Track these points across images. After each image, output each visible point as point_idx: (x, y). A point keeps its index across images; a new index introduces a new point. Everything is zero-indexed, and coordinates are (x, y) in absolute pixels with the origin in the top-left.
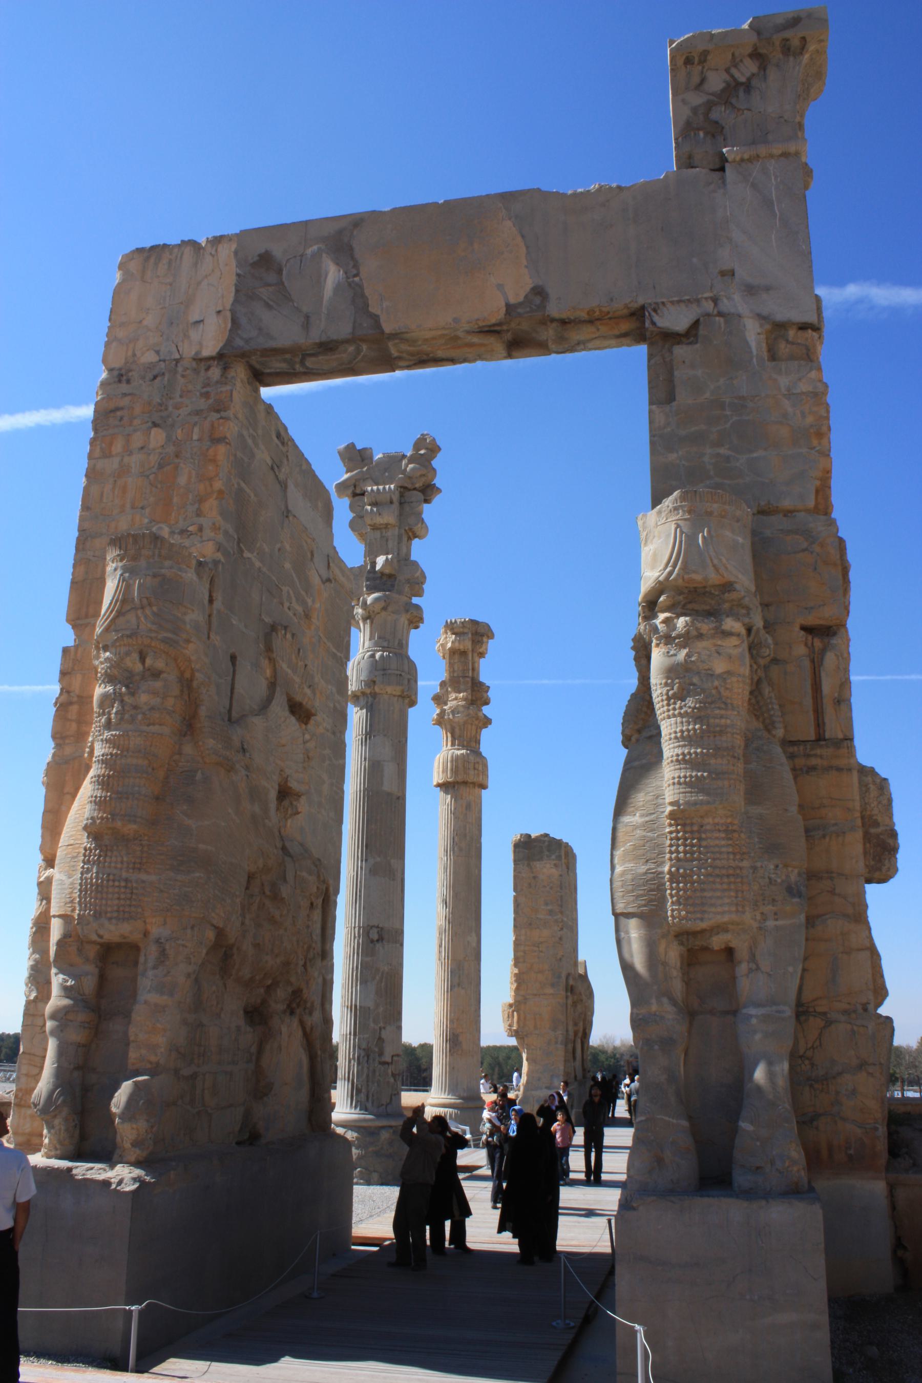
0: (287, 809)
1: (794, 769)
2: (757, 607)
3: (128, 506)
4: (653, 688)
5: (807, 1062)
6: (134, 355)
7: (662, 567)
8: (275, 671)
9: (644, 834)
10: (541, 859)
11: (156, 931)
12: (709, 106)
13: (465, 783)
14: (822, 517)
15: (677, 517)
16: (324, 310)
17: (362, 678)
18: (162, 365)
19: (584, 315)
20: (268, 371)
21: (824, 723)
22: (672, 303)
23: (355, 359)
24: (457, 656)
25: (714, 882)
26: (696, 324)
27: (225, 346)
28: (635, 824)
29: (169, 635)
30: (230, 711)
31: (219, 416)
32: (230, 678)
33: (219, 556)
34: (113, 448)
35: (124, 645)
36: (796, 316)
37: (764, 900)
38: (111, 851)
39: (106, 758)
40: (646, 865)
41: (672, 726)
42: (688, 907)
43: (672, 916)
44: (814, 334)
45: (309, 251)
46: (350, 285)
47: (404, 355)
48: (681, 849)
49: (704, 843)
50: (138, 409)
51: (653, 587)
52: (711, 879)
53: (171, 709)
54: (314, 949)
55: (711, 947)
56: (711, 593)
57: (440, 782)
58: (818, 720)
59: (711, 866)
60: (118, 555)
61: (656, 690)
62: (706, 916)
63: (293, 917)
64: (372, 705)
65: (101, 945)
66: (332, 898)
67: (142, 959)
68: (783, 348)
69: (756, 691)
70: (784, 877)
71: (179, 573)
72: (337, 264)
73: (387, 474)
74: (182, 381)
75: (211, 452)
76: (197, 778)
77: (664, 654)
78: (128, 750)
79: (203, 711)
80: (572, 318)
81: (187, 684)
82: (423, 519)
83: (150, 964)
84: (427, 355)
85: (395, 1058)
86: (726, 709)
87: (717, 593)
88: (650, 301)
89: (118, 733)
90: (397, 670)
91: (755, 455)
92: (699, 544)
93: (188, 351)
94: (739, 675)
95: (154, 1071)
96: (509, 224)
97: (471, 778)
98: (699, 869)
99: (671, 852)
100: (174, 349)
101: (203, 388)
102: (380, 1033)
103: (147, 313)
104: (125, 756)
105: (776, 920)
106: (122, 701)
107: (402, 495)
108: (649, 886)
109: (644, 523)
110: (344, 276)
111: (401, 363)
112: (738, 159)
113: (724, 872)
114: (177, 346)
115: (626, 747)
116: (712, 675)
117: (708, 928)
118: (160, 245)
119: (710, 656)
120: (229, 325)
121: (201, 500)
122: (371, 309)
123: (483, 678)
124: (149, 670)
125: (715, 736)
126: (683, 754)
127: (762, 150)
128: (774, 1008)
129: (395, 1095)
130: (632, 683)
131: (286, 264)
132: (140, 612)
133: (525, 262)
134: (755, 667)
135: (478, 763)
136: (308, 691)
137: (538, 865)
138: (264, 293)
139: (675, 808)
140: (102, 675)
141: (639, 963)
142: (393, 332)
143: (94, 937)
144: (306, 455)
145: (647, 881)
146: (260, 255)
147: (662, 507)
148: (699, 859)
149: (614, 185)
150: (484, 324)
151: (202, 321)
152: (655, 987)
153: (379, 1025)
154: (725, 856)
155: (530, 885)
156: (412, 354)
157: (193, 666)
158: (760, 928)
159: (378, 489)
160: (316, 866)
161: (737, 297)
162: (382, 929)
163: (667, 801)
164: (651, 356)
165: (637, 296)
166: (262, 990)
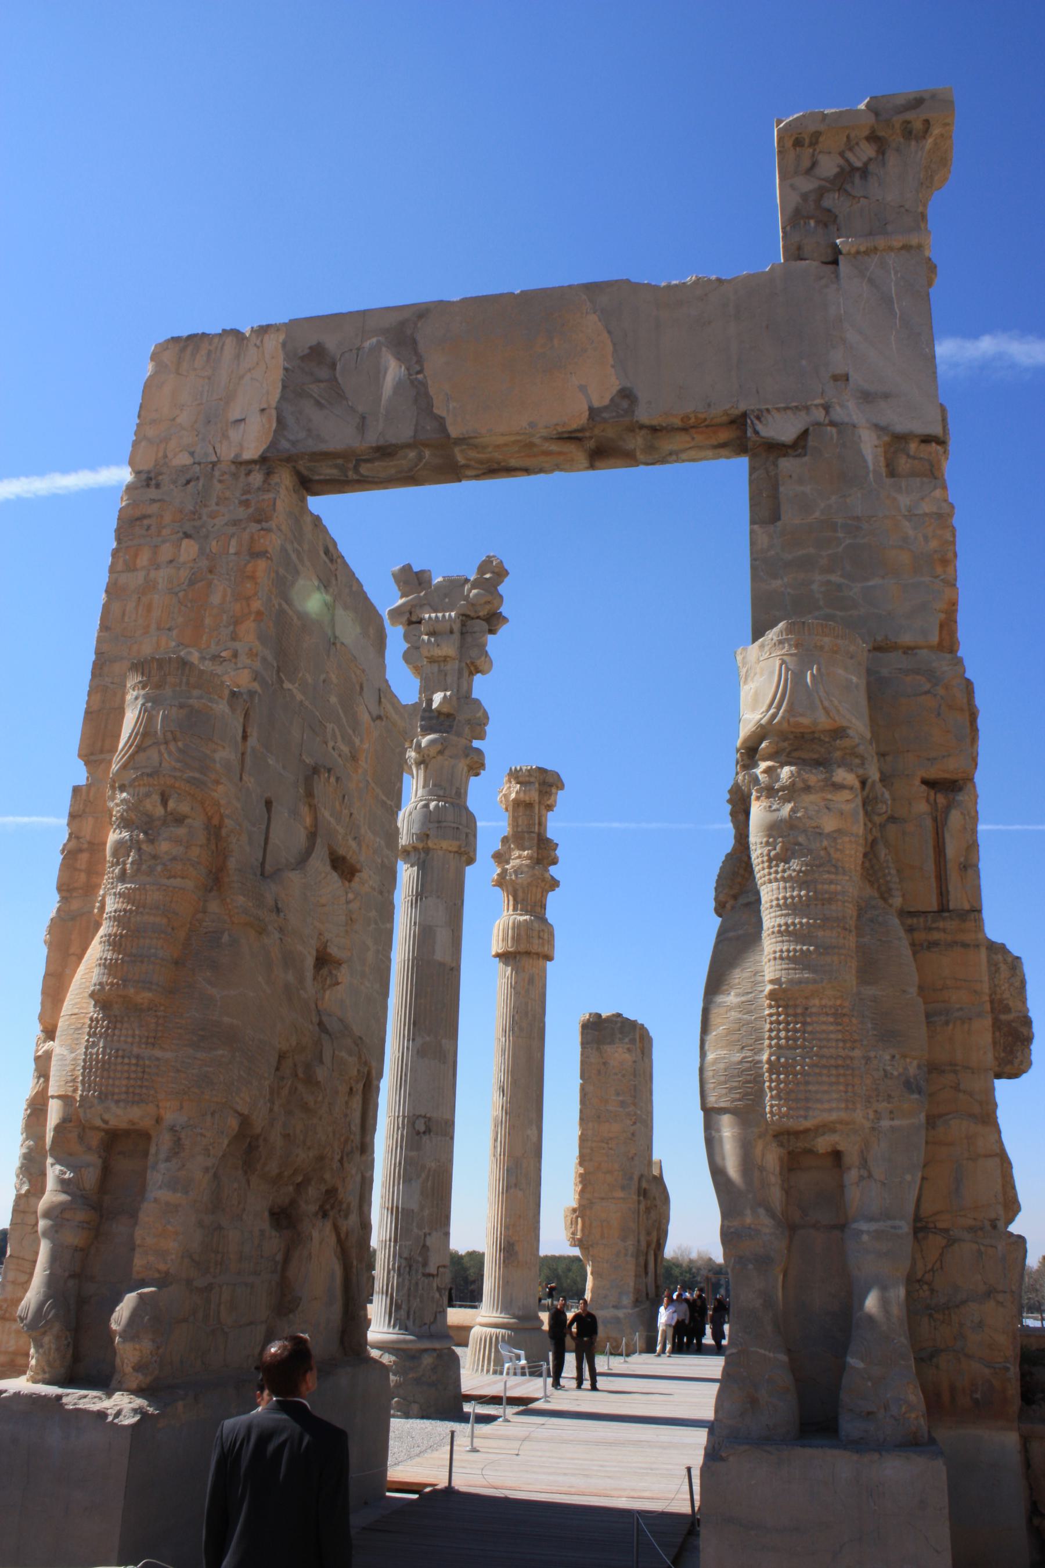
0: (326, 979)
1: (913, 945)
2: (873, 757)
4: (752, 847)
5: (925, 1287)
6: (165, 456)
7: (764, 709)
8: (316, 818)
9: (740, 1016)
10: (612, 1042)
11: (170, 1117)
12: (821, 192)
13: (528, 953)
14: (948, 656)
15: (783, 652)
16: (382, 411)
17: (413, 831)
18: (197, 468)
19: (677, 422)
20: (317, 478)
21: (948, 892)
22: (778, 409)
23: (416, 467)
24: (521, 809)
25: (820, 1074)
26: (805, 433)
27: (269, 447)
28: (729, 1004)
29: (197, 775)
30: (263, 864)
31: (260, 528)
32: (264, 827)
33: (256, 686)
34: (138, 561)
35: (144, 785)
36: (920, 428)
37: (878, 1096)
38: (122, 1022)
39: (119, 915)
40: (742, 1053)
41: (774, 892)
42: (790, 1102)
43: (771, 1112)
44: (939, 448)
45: (367, 344)
46: (412, 382)
47: (472, 463)
48: (783, 1034)
49: (809, 1028)
50: (168, 518)
51: (754, 732)
52: (817, 1070)
53: (196, 860)
54: (352, 1141)
55: (815, 1149)
56: (820, 740)
57: (500, 951)
58: (941, 888)
59: (816, 1055)
60: (140, 682)
61: (756, 850)
62: (811, 1113)
63: (330, 1104)
64: (424, 862)
65: (107, 1131)
66: (375, 1083)
67: (153, 1150)
68: (903, 464)
69: (870, 853)
70: (901, 1070)
71: (210, 704)
72: (399, 359)
73: (447, 600)
74: (218, 486)
75: (249, 568)
76: (223, 940)
77: (765, 808)
78: (144, 907)
79: (232, 864)
80: (664, 425)
81: (215, 832)
82: (486, 652)
83: (162, 1156)
84: (499, 463)
85: (440, 1269)
86: (836, 873)
87: (827, 740)
88: (752, 407)
89: (133, 886)
90: (454, 823)
91: (871, 583)
92: (807, 683)
93: (227, 453)
94: (852, 834)
95: (163, 1281)
96: (593, 318)
97: (535, 948)
98: (803, 1058)
99: (770, 1038)
100: (211, 450)
101: (243, 495)
102: (424, 1240)
103: (182, 410)
104: (141, 913)
105: (892, 1119)
106: (139, 849)
107: (463, 624)
108: (744, 1077)
109: (744, 658)
110: (406, 372)
111: (469, 473)
112: (853, 250)
113: (832, 1062)
114: (214, 448)
115: (720, 915)
116: (820, 834)
117: (812, 1128)
118: (198, 334)
119: (818, 811)
120: (274, 425)
121: (236, 622)
122: (435, 411)
124: (171, 814)
125: (823, 905)
126: (786, 924)
127: (881, 242)
128: (889, 1223)
129: (440, 1312)
130: (728, 843)
131: (340, 359)
132: (163, 748)
133: (611, 361)
134: (870, 825)
135: (543, 930)
136: (353, 844)
137: (608, 1049)
139: (776, 987)
140: (117, 819)
141: (732, 1167)
142: (461, 436)
143: (98, 1123)
144: (357, 575)
145: (742, 1071)
146: (311, 348)
147: (765, 641)
148: (803, 1047)
149: (713, 277)
150: (564, 430)
151: (244, 420)
152: (750, 1196)
153: (424, 1231)
154: (834, 1044)
155: (599, 1072)
156: (481, 462)
157: (222, 811)
158: (873, 1129)
159: (437, 617)
160: (357, 1045)
161: (851, 404)
162: (430, 1119)
163: (767, 978)
164: (752, 470)
165: (738, 401)
166: (291, 1188)
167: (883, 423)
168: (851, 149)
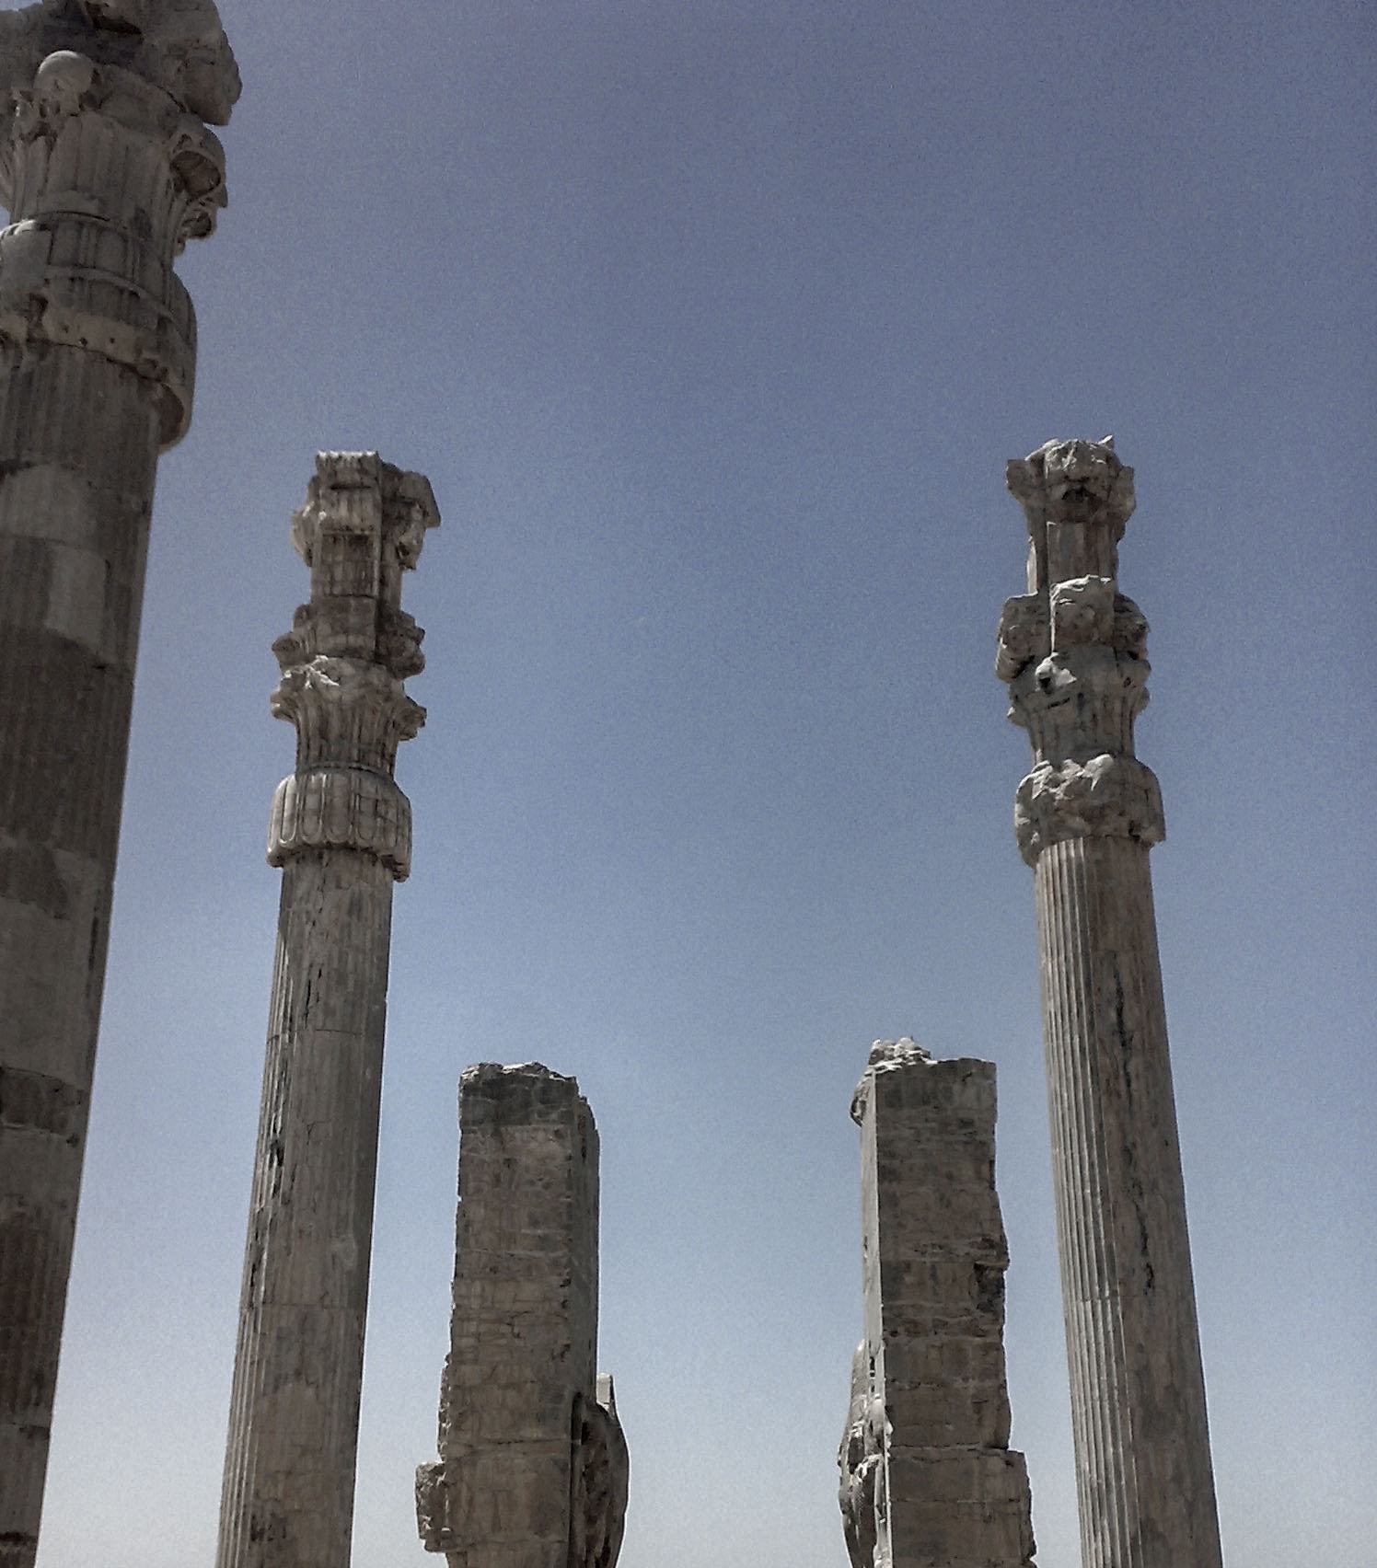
10: (525, 1120)
13: (349, 849)
90: (122, 276)
97: (366, 835)
137: (517, 1133)
155: (497, 1180)
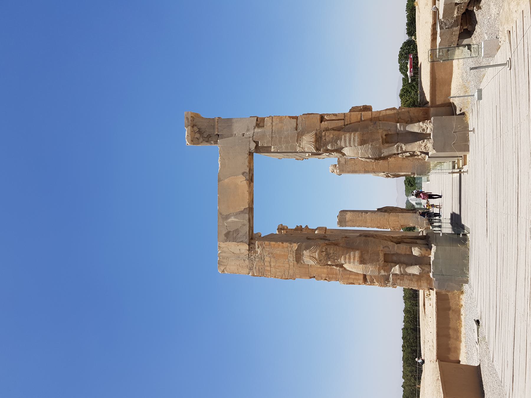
3: (284, 265)
6: (246, 266)
11: (381, 248)
12: (203, 137)
26: (254, 141)
27: (247, 244)
34: (269, 270)
50: (260, 264)
113: (371, 135)
123: (294, 227)
127: (216, 127)
138: (235, 235)
146: (225, 237)
155: (353, 222)
167: (254, 128)
168: (194, 131)
